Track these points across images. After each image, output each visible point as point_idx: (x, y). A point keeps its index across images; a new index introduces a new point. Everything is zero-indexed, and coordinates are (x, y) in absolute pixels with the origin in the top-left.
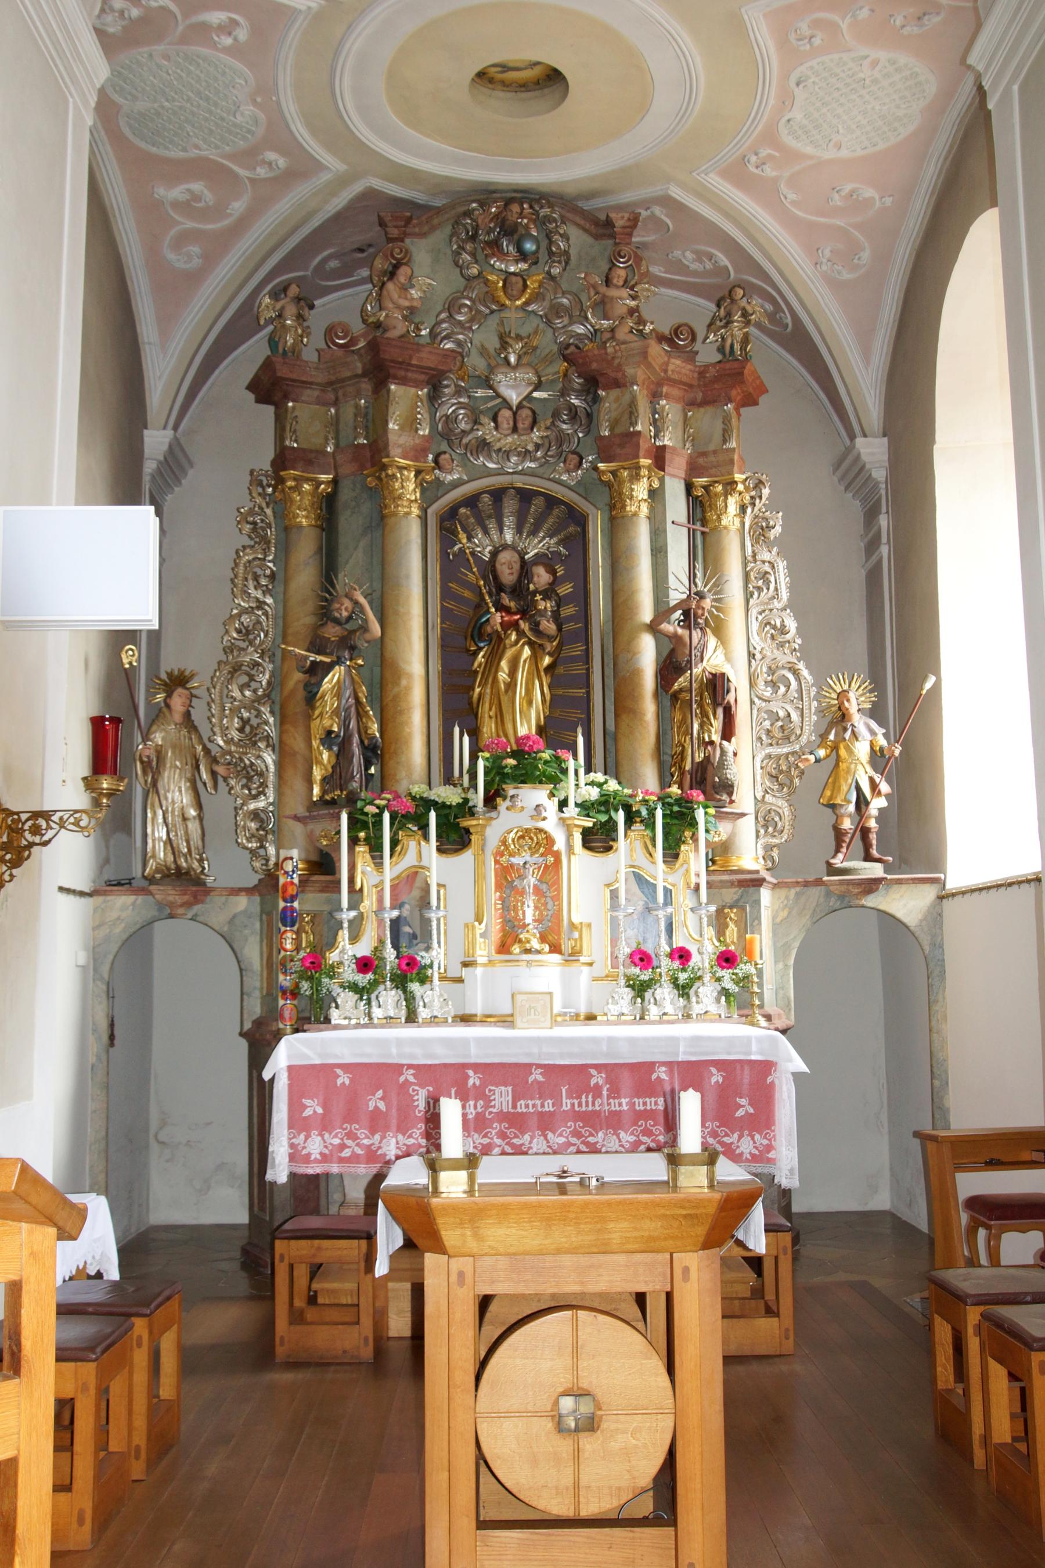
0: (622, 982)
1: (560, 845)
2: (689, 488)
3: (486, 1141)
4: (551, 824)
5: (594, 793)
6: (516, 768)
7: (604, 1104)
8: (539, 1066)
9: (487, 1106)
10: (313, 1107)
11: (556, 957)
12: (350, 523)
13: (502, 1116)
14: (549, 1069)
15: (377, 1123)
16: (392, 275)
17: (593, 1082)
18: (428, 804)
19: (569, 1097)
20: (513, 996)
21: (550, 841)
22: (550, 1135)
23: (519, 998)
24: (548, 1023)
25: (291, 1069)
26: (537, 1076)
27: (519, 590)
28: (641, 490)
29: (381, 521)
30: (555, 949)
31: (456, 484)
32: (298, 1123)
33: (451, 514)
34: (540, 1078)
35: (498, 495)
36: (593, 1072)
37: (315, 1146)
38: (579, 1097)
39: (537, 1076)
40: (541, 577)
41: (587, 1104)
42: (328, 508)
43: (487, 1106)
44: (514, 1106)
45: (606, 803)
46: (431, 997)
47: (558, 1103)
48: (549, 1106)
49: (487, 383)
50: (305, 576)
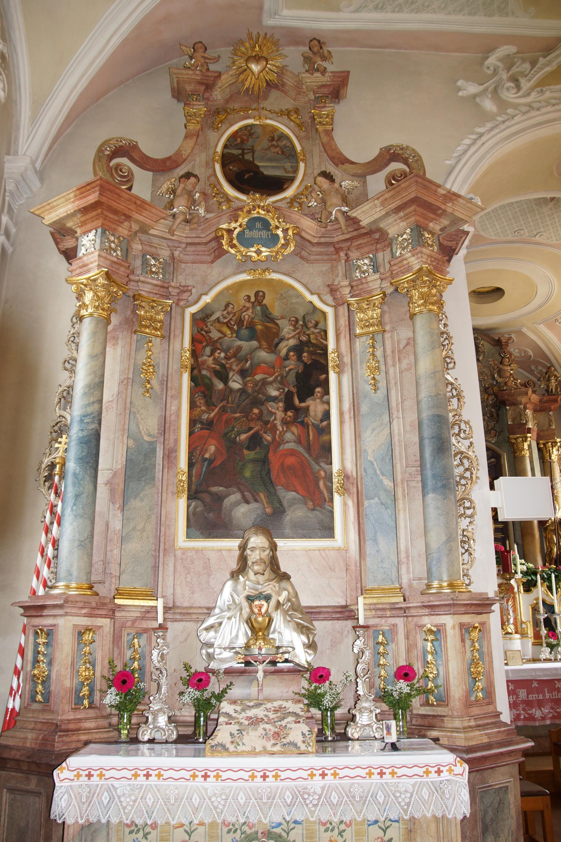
0: (545, 645)
2: (538, 444)
3: (518, 712)
5: (524, 568)
8: (536, 680)
9: (517, 698)
11: (518, 636)
13: (523, 702)
14: (539, 681)
17: (557, 686)
19: (548, 693)
20: (505, 653)
22: (542, 709)
23: (508, 653)
24: (521, 663)
26: (535, 684)
28: (526, 446)
34: (537, 685)
36: (556, 682)
38: (552, 693)
39: (535, 684)
43: (517, 698)
44: (528, 697)
47: (544, 695)
48: (541, 697)
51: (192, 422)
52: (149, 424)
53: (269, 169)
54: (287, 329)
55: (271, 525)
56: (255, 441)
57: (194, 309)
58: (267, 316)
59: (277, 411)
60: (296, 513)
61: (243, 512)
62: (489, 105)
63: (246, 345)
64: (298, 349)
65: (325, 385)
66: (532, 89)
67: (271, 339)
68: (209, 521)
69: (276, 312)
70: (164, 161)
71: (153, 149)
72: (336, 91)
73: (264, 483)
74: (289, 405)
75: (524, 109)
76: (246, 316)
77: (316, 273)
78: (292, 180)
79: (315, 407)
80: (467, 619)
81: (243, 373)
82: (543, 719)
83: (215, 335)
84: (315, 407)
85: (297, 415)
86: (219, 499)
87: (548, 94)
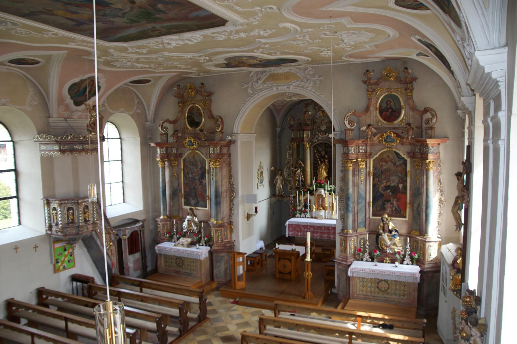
1: (324, 196)
4: (323, 193)
6: (320, 185)
7: (323, 231)
10: (291, 229)
12: (301, 149)
15: (298, 231)
16: (305, 113)
18: (309, 190)
21: (323, 196)
25: (288, 225)
27: (324, 157)
29: (304, 150)
30: (324, 209)
31: (316, 142)
32: (289, 230)
33: (315, 147)
35: (321, 143)
37: (291, 233)
40: (326, 156)
41: (322, 231)
42: (298, 146)
45: (331, 190)
46: (308, 215)
49: (319, 127)
50: (295, 156)
51: (184, 183)
52: (176, 184)
53: (197, 121)
54: (199, 164)
55: (197, 205)
56: (194, 188)
57: (183, 158)
58: (196, 161)
59: (198, 182)
60: (201, 203)
61: (193, 202)
62: (250, 91)
63: (192, 167)
64: (201, 169)
65: (206, 176)
66: (262, 84)
67: (196, 166)
68: (187, 204)
69: (197, 159)
70: (174, 121)
71: (171, 119)
72: (210, 94)
73: (196, 197)
74: (200, 181)
75: (259, 91)
76: (192, 160)
77: (204, 150)
78: (201, 123)
79: (204, 182)
80: (217, 229)
81: (192, 173)
82: (317, 237)
83: (187, 165)
84: (203, 181)
85: (201, 183)
86: (189, 199)
87: (265, 85)
